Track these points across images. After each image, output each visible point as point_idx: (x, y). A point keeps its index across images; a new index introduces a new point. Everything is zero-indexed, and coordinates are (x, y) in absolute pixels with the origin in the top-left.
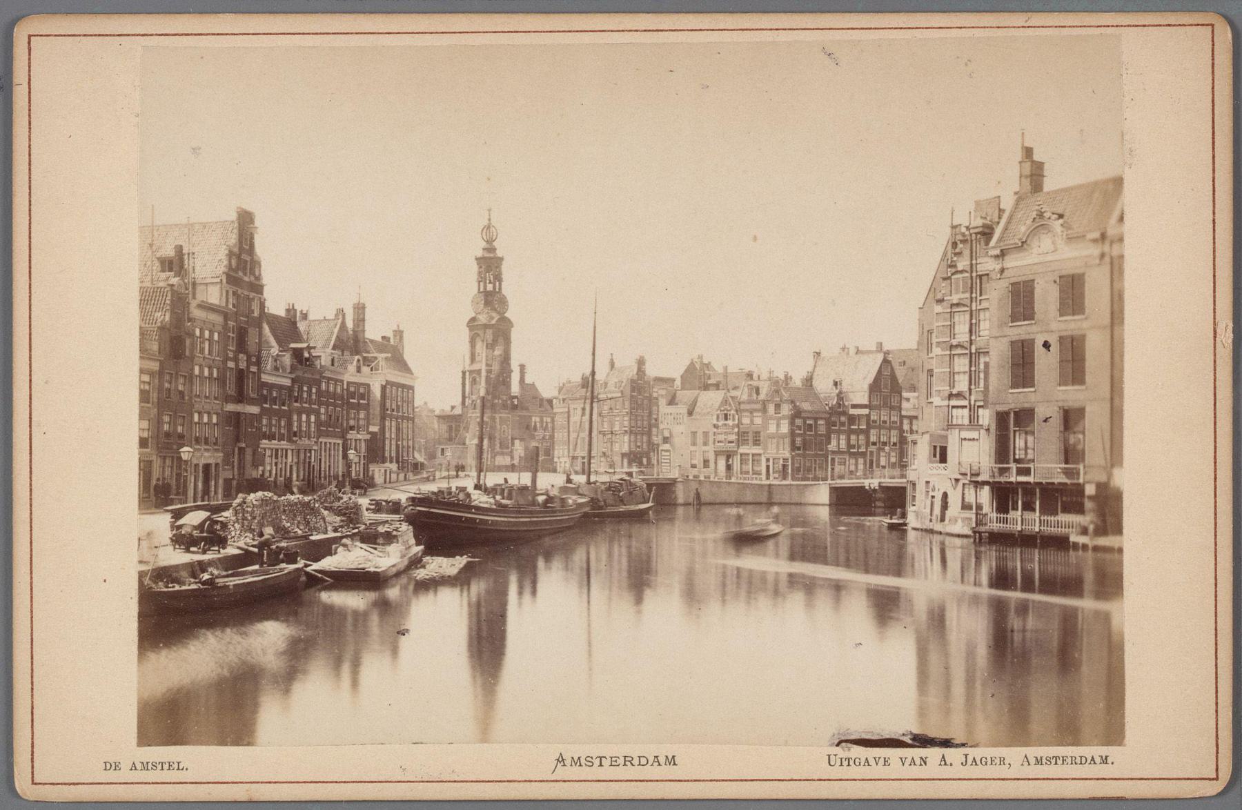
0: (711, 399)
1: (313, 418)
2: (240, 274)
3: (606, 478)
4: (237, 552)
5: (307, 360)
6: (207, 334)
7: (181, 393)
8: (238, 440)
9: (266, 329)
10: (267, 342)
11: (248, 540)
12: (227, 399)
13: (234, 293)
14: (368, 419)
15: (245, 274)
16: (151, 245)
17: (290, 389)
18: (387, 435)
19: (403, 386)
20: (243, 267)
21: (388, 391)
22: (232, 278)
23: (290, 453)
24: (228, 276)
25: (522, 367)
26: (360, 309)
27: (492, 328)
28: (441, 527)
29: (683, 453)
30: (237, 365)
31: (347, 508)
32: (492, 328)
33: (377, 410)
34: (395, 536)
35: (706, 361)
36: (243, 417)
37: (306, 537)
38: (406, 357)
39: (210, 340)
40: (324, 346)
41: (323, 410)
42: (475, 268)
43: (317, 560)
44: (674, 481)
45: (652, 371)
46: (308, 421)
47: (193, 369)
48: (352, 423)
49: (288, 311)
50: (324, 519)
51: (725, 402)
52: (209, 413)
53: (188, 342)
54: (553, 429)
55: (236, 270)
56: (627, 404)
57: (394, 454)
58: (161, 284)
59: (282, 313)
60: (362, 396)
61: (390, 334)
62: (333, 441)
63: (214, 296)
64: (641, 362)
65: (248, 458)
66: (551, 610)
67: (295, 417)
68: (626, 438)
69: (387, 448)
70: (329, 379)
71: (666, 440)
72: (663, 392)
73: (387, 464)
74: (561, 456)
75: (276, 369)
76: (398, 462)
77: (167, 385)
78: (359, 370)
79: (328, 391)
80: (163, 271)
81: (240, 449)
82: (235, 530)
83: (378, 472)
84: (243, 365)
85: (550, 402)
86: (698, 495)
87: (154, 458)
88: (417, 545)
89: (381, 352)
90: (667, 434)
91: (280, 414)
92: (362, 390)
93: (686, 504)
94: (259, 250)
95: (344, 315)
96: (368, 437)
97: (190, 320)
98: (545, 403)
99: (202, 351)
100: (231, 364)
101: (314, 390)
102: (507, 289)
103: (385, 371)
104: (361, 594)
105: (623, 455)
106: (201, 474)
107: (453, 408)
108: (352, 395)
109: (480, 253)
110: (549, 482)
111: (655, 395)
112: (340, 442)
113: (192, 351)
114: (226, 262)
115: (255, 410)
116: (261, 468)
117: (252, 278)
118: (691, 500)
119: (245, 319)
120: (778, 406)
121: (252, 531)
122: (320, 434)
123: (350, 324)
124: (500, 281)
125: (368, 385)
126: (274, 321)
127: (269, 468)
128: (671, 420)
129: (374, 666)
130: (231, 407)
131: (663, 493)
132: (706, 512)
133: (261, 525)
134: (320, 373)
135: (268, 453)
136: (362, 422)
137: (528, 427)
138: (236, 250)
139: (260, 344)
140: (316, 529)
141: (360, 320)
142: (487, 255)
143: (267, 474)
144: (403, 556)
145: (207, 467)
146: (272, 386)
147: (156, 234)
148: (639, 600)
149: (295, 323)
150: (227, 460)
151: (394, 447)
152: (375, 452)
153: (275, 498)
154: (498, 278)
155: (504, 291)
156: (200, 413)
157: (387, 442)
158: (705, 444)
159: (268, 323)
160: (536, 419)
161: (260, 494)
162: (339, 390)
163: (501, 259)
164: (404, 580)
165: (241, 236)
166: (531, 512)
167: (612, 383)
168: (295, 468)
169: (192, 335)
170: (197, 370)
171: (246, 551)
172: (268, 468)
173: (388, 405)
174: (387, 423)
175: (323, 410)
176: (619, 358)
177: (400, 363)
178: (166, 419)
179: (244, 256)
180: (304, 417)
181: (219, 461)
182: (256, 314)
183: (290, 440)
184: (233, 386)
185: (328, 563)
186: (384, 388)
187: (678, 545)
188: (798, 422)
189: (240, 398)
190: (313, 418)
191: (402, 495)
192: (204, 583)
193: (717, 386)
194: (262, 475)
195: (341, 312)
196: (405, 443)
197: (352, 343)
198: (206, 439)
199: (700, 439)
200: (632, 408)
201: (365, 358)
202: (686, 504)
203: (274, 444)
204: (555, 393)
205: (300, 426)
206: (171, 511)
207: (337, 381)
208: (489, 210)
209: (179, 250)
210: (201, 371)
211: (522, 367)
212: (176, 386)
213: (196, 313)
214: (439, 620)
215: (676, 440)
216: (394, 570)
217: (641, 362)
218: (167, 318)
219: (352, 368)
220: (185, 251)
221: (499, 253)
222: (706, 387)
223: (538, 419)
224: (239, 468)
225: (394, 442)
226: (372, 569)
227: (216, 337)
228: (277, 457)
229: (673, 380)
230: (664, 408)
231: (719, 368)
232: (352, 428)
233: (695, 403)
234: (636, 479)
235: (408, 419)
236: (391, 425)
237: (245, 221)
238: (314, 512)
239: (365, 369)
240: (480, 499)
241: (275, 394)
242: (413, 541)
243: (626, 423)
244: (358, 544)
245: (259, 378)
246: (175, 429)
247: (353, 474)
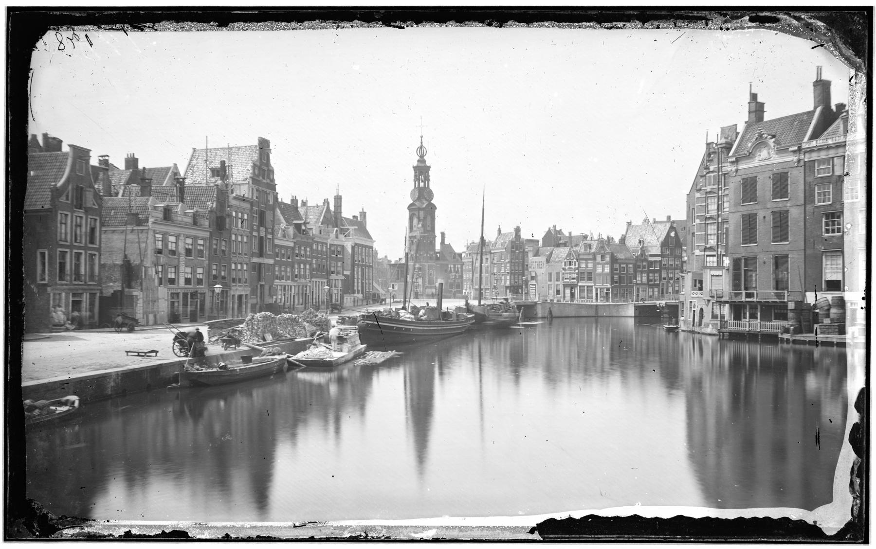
0: (561, 253)
1: (308, 267)
2: (261, 178)
3: (490, 302)
4: (247, 348)
5: (304, 231)
6: (240, 215)
7: (224, 251)
8: (259, 280)
9: (278, 212)
10: (279, 220)
12: (253, 255)
13: (257, 190)
16: (206, 161)
17: (293, 249)
19: (366, 247)
22: (255, 180)
24: (252, 178)
25: (443, 234)
27: (423, 208)
32: (423, 208)
33: (348, 262)
35: (558, 229)
36: (263, 266)
37: (292, 340)
38: (368, 228)
40: (316, 222)
44: (536, 303)
45: (525, 235)
46: (305, 268)
47: (231, 237)
48: (333, 269)
49: (292, 200)
51: (570, 254)
52: (241, 264)
53: (227, 220)
55: (258, 176)
57: (360, 288)
58: (212, 185)
59: (289, 202)
62: (320, 280)
63: (244, 191)
64: (518, 230)
66: (460, 385)
67: (296, 266)
68: (508, 277)
69: (356, 284)
70: (318, 242)
71: (533, 278)
72: (531, 249)
73: (356, 295)
74: (468, 289)
75: (284, 236)
77: (214, 247)
78: (337, 237)
79: (317, 250)
80: (213, 176)
83: (348, 300)
84: (263, 234)
85: (460, 255)
87: (207, 291)
88: (362, 344)
90: (533, 274)
91: (286, 264)
92: (339, 249)
93: (543, 318)
95: (328, 203)
96: (343, 278)
98: (457, 257)
99: (237, 226)
100: (255, 234)
102: (432, 186)
104: (322, 374)
105: (507, 287)
108: (333, 252)
109: (415, 164)
110: (450, 305)
113: (230, 225)
115: (271, 261)
118: (546, 315)
120: (603, 257)
121: (258, 336)
123: (332, 208)
124: (429, 180)
125: (343, 246)
126: (284, 207)
128: (536, 265)
130: (255, 260)
131: (528, 311)
132: (555, 321)
133: (264, 332)
135: (279, 288)
137: (446, 271)
138: (258, 163)
139: (273, 221)
140: (299, 334)
142: (420, 165)
143: (279, 301)
144: (349, 351)
145: (240, 297)
146: (281, 247)
149: (297, 208)
150: (254, 292)
151: (360, 284)
152: (348, 287)
154: (427, 179)
155: (431, 187)
156: (235, 263)
158: (558, 280)
159: (280, 210)
161: (263, 313)
162: (324, 249)
163: (430, 167)
164: (350, 365)
165: (261, 154)
169: (230, 216)
170: (233, 237)
171: (253, 349)
173: (356, 258)
175: (314, 262)
176: (499, 225)
178: (214, 267)
180: (302, 266)
181: (248, 293)
183: (293, 280)
184: (257, 246)
185: (301, 356)
186: (353, 248)
187: (538, 342)
188: (616, 266)
189: (261, 254)
190: (308, 267)
192: (221, 368)
193: (565, 245)
194: (276, 302)
195: (326, 202)
197: (333, 218)
198: (240, 280)
199: (554, 277)
202: (543, 318)
204: (465, 249)
205: (299, 271)
206: (208, 324)
207: (323, 243)
211: (443, 234)
212: (221, 247)
214: (390, 389)
215: (539, 278)
216: (343, 359)
217: (518, 230)
219: (333, 235)
220: (227, 164)
221: (428, 164)
222: (558, 245)
224: (261, 297)
227: (246, 217)
229: (538, 241)
230: (531, 258)
232: (333, 272)
233: (551, 254)
234: (512, 303)
235: (369, 266)
237: (264, 146)
238: (300, 325)
239: (341, 237)
240: (405, 315)
242: (359, 342)
245: (273, 242)
246: (220, 273)
247: (334, 301)
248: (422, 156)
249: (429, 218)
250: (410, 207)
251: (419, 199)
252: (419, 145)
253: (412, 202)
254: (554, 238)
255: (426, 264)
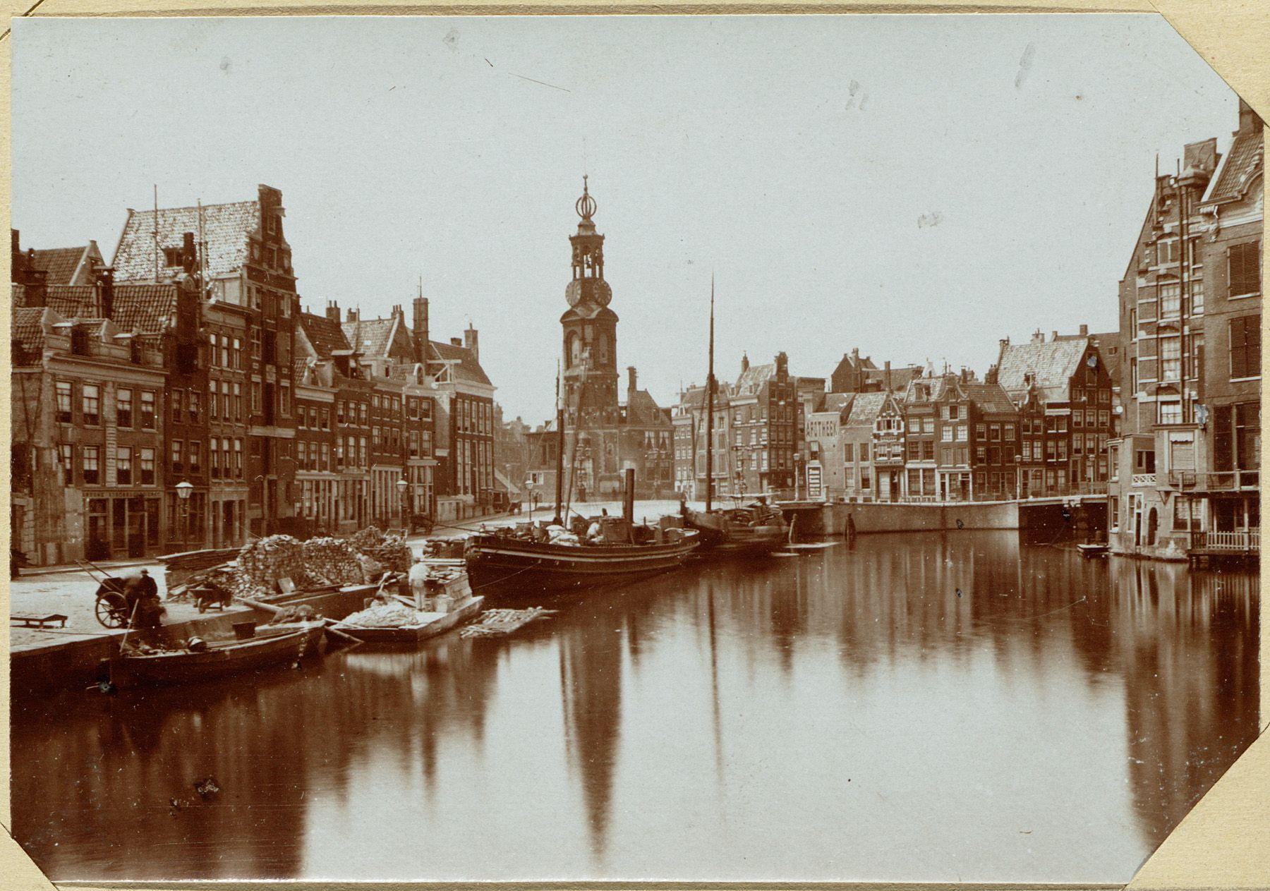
1: (363, 442)
2: (265, 266)
3: (729, 505)
4: (244, 609)
5: (354, 370)
6: (225, 340)
7: (193, 415)
8: (266, 471)
9: (301, 333)
10: (304, 349)
11: (260, 595)
12: (252, 422)
13: (258, 291)
15: (271, 267)
16: (155, 233)
17: (333, 407)
18: (460, 460)
19: (478, 399)
21: (459, 406)
22: (254, 270)
23: (334, 485)
24: (249, 268)
25: (632, 372)
26: (421, 306)
27: (591, 321)
28: (517, 575)
29: (835, 473)
30: (264, 379)
31: (391, 552)
32: (591, 321)
34: (442, 585)
35: (862, 356)
36: (272, 443)
37: (334, 589)
38: (481, 363)
40: (378, 353)
44: (821, 505)
47: (207, 386)
48: (413, 446)
49: (329, 310)
51: (887, 406)
52: (230, 439)
53: (200, 352)
55: (260, 262)
56: (765, 412)
57: (468, 483)
58: (167, 282)
59: (322, 313)
61: (462, 336)
63: (233, 295)
64: (782, 360)
67: (340, 441)
68: (765, 455)
69: (460, 475)
71: (814, 455)
72: (809, 396)
73: (461, 496)
74: (684, 480)
75: (314, 382)
76: (474, 493)
77: (175, 406)
78: (420, 382)
80: (170, 264)
81: (271, 483)
83: (445, 507)
84: (271, 379)
85: (667, 412)
86: (851, 523)
87: (161, 495)
88: (475, 594)
90: (815, 448)
91: (320, 438)
94: (289, 235)
95: (402, 314)
96: (435, 463)
99: (219, 362)
100: (256, 378)
101: (363, 407)
102: (610, 275)
104: (395, 657)
105: (762, 475)
106: (222, 514)
107: (547, 423)
109: (574, 232)
110: (648, 512)
114: (245, 253)
115: (289, 433)
116: (298, 505)
117: (281, 272)
118: (842, 529)
120: (954, 411)
121: (265, 583)
123: (409, 324)
124: (601, 264)
127: (307, 504)
128: (820, 427)
130: (257, 431)
131: (807, 522)
132: (862, 541)
133: (277, 576)
135: (307, 485)
136: (426, 445)
137: (640, 444)
138: (259, 237)
139: (292, 352)
140: (348, 578)
142: (584, 233)
143: (306, 512)
144: (450, 610)
145: (229, 505)
146: (308, 403)
147: (161, 221)
149: (339, 324)
150: (255, 494)
151: (468, 475)
152: (445, 481)
153: (295, 542)
154: (598, 260)
155: (607, 278)
157: (460, 468)
158: (864, 458)
161: (275, 537)
162: (396, 406)
164: (453, 638)
166: (625, 550)
169: (206, 342)
170: (213, 386)
171: (257, 610)
173: (460, 423)
174: (459, 445)
175: (375, 432)
176: (745, 353)
178: (176, 447)
179: (270, 245)
180: (352, 441)
182: (287, 314)
184: (260, 404)
185: (355, 620)
186: (453, 402)
187: (826, 584)
188: (981, 428)
189: (269, 418)
190: (363, 442)
193: (877, 387)
194: (300, 513)
195: (398, 312)
196: (483, 469)
197: (412, 345)
200: (771, 417)
201: (430, 365)
202: (836, 535)
204: (677, 401)
205: (346, 452)
206: (166, 561)
208: (586, 178)
209: (188, 238)
210: (219, 387)
211: (632, 372)
212: (188, 405)
214: (533, 682)
215: (827, 455)
216: (439, 625)
217: (782, 360)
218: (173, 324)
219: (412, 378)
220: (196, 240)
221: (599, 231)
222: (864, 389)
223: (652, 435)
224: (270, 506)
225: (468, 468)
226: (408, 627)
227: (236, 344)
228: (317, 491)
229: (823, 381)
230: (810, 415)
232: (414, 453)
233: (850, 406)
234: (773, 505)
235: (486, 439)
237: (270, 202)
240: (561, 536)
241: (313, 413)
242: (469, 590)
244: (396, 596)
245: (293, 394)
246: (187, 459)
247: (417, 510)
248: (587, 217)
249: (603, 340)
250: (566, 319)
251: (583, 301)
252: (581, 194)
253: (569, 308)
254: (854, 376)
255: (600, 432)
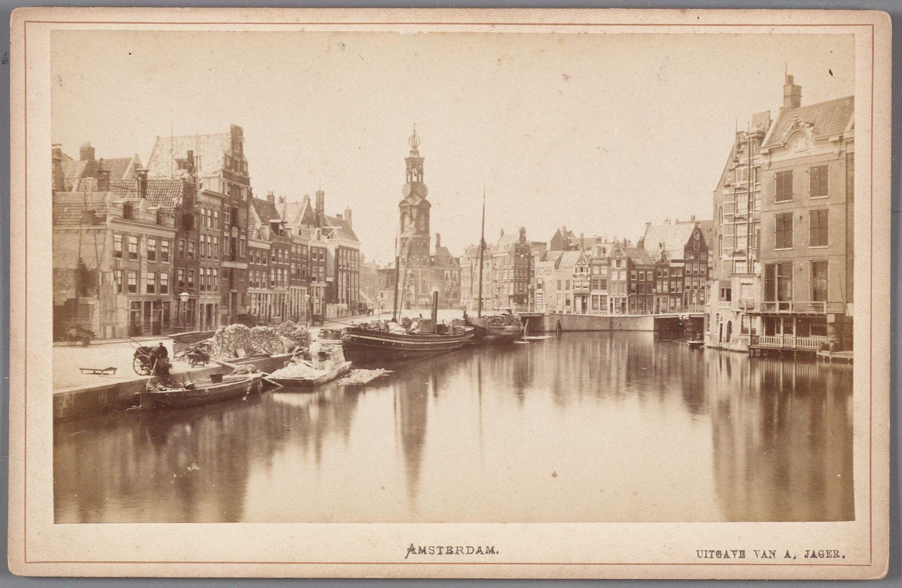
0: (571, 257)
1: (286, 272)
2: (233, 171)
3: (491, 314)
5: (282, 231)
7: (191, 254)
8: (231, 287)
10: (253, 218)
11: (225, 358)
12: (224, 259)
13: (229, 184)
14: (325, 272)
15: (236, 171)
16: (171, 150)
17: (269, 251)
18: (340, 284)
19: (351, 249)
20: (235, 169)
21: (340, 253)
22: (227, 174)
23: (269, 296)
25: (438, 236)
26: (320, 195)
27: (416, 208)
30: (231, 235)
31: (300, 335)
32: (416, 208)
33: (331, 266)
34: (328, 355)
35: (568, 230)
37: (267, 356)
38: (354, 229)
39: (212, 217)
41: (293, 267)
42: (405, 165)
43: (271, 372)
44: (543, 315)
45: (530, 238)
46: (282, 275)
47: (199, 238)
48: (314, 275)
49: (269, 196)
50: (282, 343)
51: (581, 259)
52: (211, 268)
53: (195, 218)
54: (460, 279)
55: (230, 168)
56: (513, 261)
57: (344, 297)
58: (178, 178)
59: (265, 199)
60: (321, 257)
61: (342, 213)
62: (300, 288)
63: (215, 186)
64: (523, 232)
65: (239, 300)
67: (273, 272)
68: (512, 285)
69: (340, 293)
70: (297, 244)
71: (539, 286)
72: (537, 252)
73: (340, 305)
75: (259, 237)
76: (347, 303)
77: (181, 249)
78: (319, 239)
79: (297, 252)
80: (179, 168)
81: (233, 294)
82: (217, 349)
83: (331, 310)
84: (235, 235)
85: (458, 260)
86: (559, 325)
87: (172, 300)
88: (347, 360)
89: (335, 225)
90: (540, 282)
91: (262, 269)
92: (321, 252)
93: (551, 332)
94: (246, 153)
95: (309, 200)
96: (325, 285)
97: (197, 203)
98: (455, 262)
100: (226, 234)
101: (286, 252)
102: (426, 180)
103: (338, 239)
104: (301, 395)
105: (510, 297)
107: (390, 264)
108: (314, 256)
109: (408, 155)
110: (446, 317)
111: (532, 254)
112: (306, 289)
113: (198, 224)
114: (222, 163)
115: (244, 266)
116: (248, 307)
117: (242, 174)
118: (554, 328)
119: (236, 202)
120: (618, 262)
122: (291, 283)
124: (422, 174)
125: (326, 249)
126: (259, 205)
127: (253, 307)
128: (543, 271)
129: (332, 443)
130: (227, 264)
131: (534, 324)
132: (565, 336)
133: (236, 347)
134: (291, 240)
135: (254, 296)
136: (321, 275)
138: (230, 154)
139: (247, 220)
141: (320, 203)
142: (413, 156)
143: (253, 311)
144: (333, 369)
145: (209, 306)
146: (256, 249)
147: (174, 143)
148: (521, 396)
149: (273, 205)
150: (225, 301)
151: (344, 293)
152: (331, 295)
153: (246, 328)
155: (425, 182)
156: (204, 268)
157: (340, 288)
158: (567, 288)
159: (255, 207)
160: (447, 272)
161: (235, 325)
164: (333, 385)
165: (233, 143)
166: (431, 338)
167: (502, 248)
168: (273, 307)
169: (198, 213)
170: (202, 238)
171: (224, 366)
172: (254, 307)
173: (340, 263)
174: (340, 275)
175: (293, 267)
177: (347, 230)
178: (180, 272)
179: (236, 158)
180: (279, 271)
181: (218, 302)
182: (245, 199)
183: (269, 287)
185: (279, 374)
186: (337, 251)
187: (545, 358)
188: (634, 273)
189: (233, 258)
190: (286, 272)
191: (340, 326)
192: (187, 388)
193: (576, 248)
194: (249, 312)
195: (307, 199)
196: (353, 289)
197: (315, 219)
198: (209, 287)
199: (564, 285)
200: (516, 264)
201: (324, 230)
202: (551, 332)
203: (258, 290)
204: (463, 253)
206: (173, 337)
207: (303, 246)
209: (190, 153)
210: (205, 239)
211: (438, 236)
213: (202, 198)
215: (547, 286)
216: (325, 379)
217: (523, 232)
218: (181, 202)
219: (314, 237)
220: (194, 155)
221: (421, 155)
222: (568, 249)
223: (449, 272)
224: (233, 308)
225: (344, 289)
226: (308, 378)
227: (216, 215)
228: (259, 299)
229: (545, 244)
230: (537, 264)
231: (578, 236)
232: (314, 279)
233: (560, 259)
234: (516, 314)
235: (355, 272)
236: (343, 277)
237: (236, 135)
238: (277, 339)
239: (324, 238)
240: (396, 329)
241: (258, 255)
242: (343, 358)
243: (512, 275)
244: (303, 361)
245: (247, 243)
246: (187, 279)
248: (415, 147)
249: (423, 217)
251: (411, 195)
254: (563, 242)
255: (420, 270)
